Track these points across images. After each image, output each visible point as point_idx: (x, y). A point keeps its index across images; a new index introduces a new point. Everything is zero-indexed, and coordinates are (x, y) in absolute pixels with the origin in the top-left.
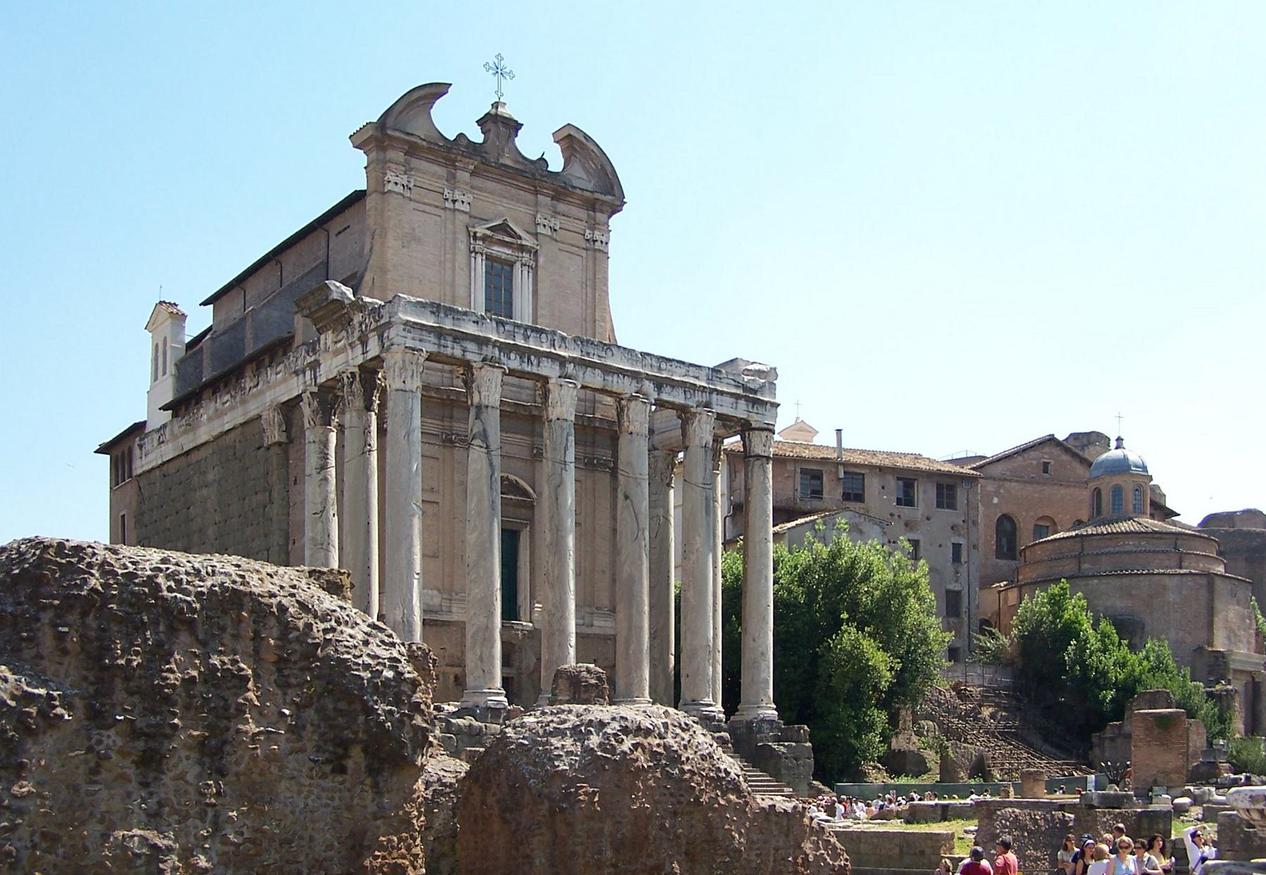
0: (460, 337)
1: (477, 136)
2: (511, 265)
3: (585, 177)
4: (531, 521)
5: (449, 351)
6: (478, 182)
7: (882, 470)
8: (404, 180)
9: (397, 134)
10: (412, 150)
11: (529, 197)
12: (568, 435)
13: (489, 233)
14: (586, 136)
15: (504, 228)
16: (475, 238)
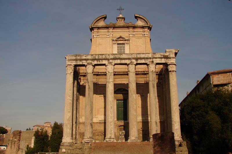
0: (81, 60)
5: (79, 64)
6: (114, 30)
12: (110, 75)
16: (114, 41)
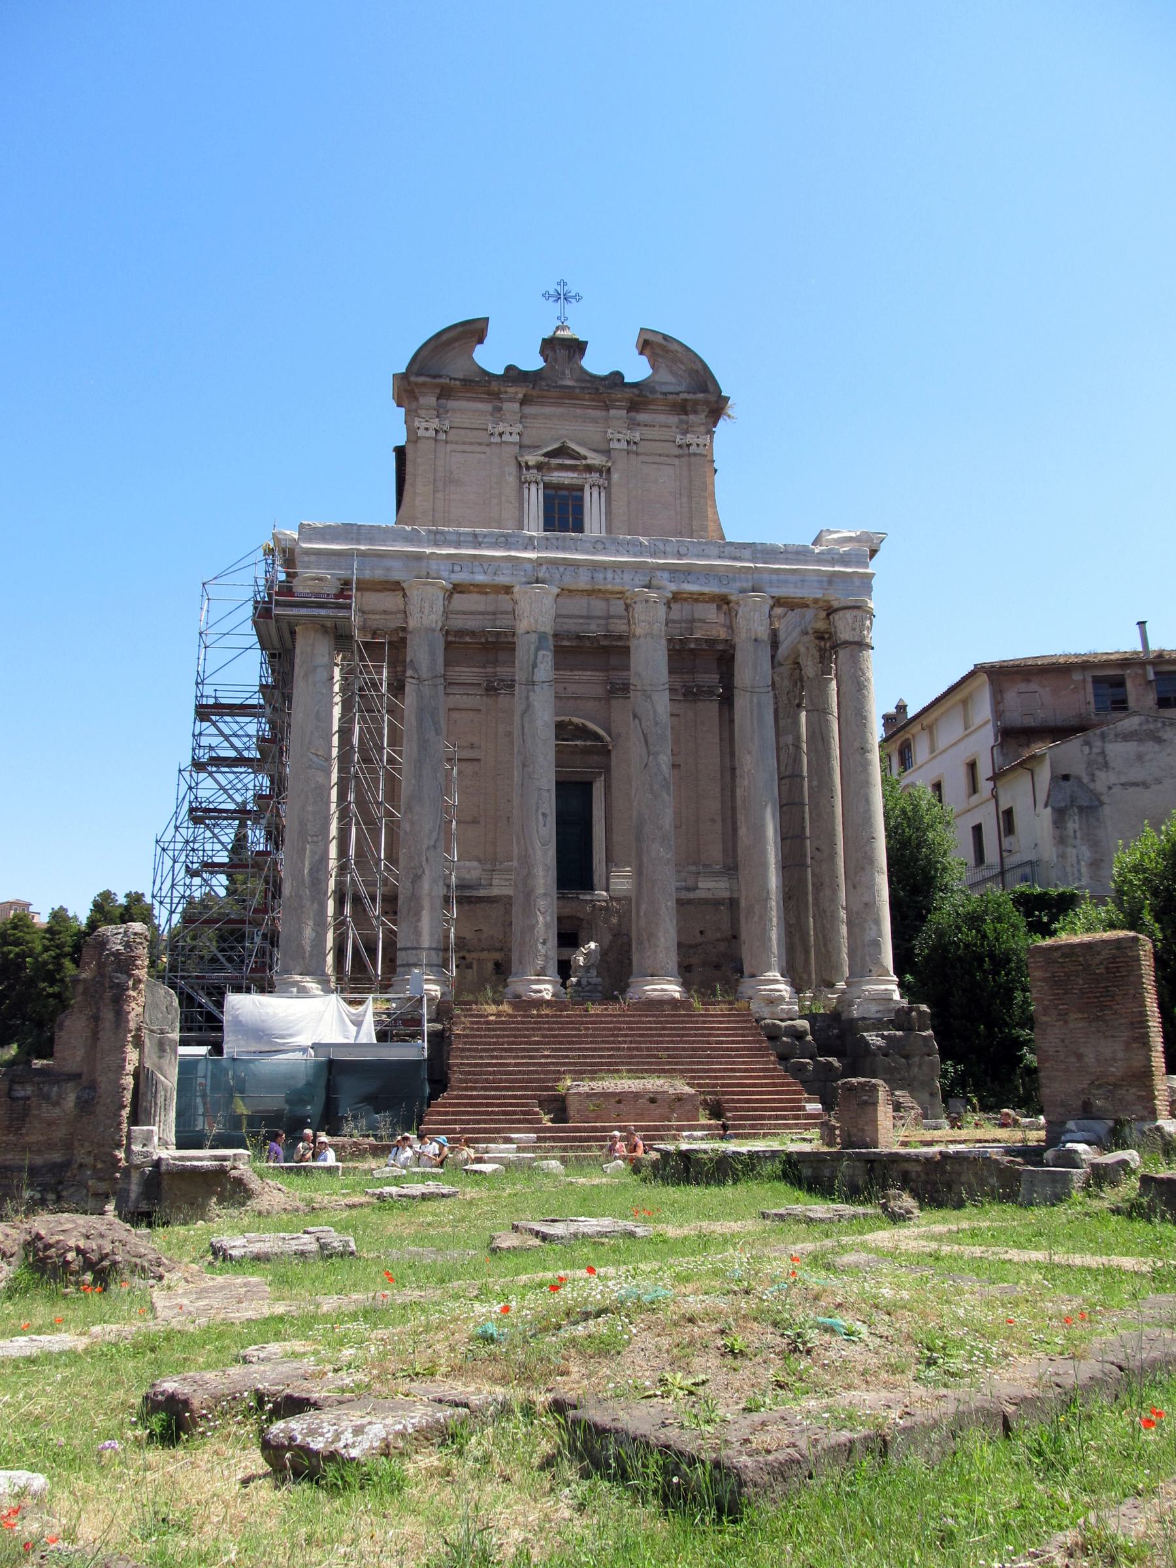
2: (582, 489)
3: (673, 380)
4: (607, 770)
6: (529, 410)
8: (435, 423)
9: (421, 379)
10: (445, 393)
12: (538, 649)
13: (542, 459)
14: (666, 337)
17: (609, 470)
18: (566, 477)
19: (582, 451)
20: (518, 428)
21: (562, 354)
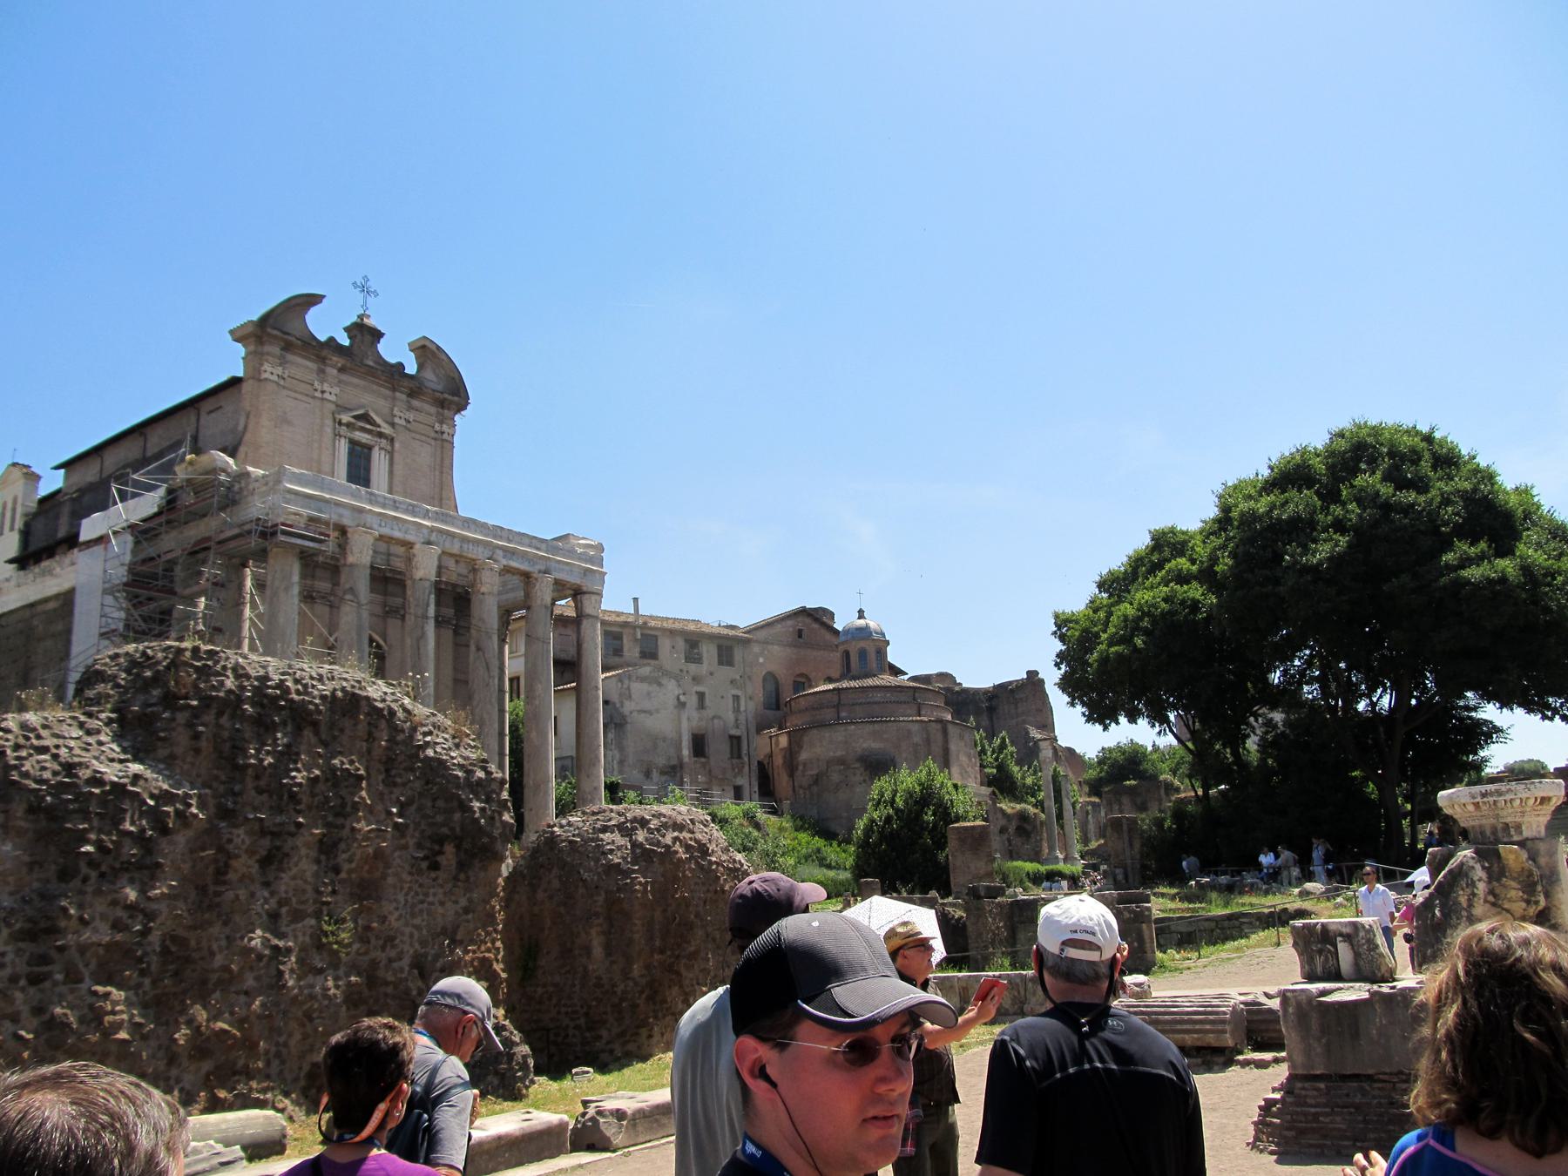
1: (346, 342)
2: (370, 448)
6: (344, 377)
7: (672, 633)
8: (279, 370)
9: (275, 332)
10: (288, 347)
11: (388, 392)
14: (438, 348)
15: (365, 417)
17: (392, 440)
18: (363, 437)
19: (378, 420)
20: (336, 390)
21: (368, 338)
